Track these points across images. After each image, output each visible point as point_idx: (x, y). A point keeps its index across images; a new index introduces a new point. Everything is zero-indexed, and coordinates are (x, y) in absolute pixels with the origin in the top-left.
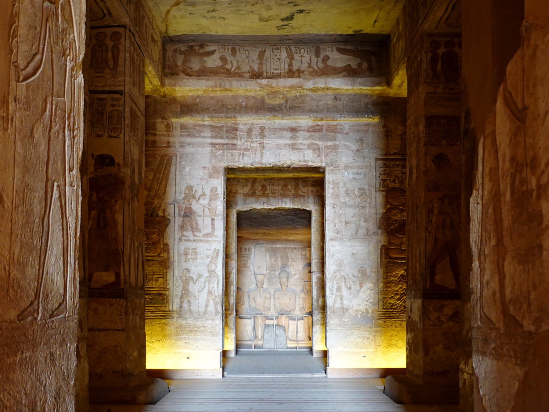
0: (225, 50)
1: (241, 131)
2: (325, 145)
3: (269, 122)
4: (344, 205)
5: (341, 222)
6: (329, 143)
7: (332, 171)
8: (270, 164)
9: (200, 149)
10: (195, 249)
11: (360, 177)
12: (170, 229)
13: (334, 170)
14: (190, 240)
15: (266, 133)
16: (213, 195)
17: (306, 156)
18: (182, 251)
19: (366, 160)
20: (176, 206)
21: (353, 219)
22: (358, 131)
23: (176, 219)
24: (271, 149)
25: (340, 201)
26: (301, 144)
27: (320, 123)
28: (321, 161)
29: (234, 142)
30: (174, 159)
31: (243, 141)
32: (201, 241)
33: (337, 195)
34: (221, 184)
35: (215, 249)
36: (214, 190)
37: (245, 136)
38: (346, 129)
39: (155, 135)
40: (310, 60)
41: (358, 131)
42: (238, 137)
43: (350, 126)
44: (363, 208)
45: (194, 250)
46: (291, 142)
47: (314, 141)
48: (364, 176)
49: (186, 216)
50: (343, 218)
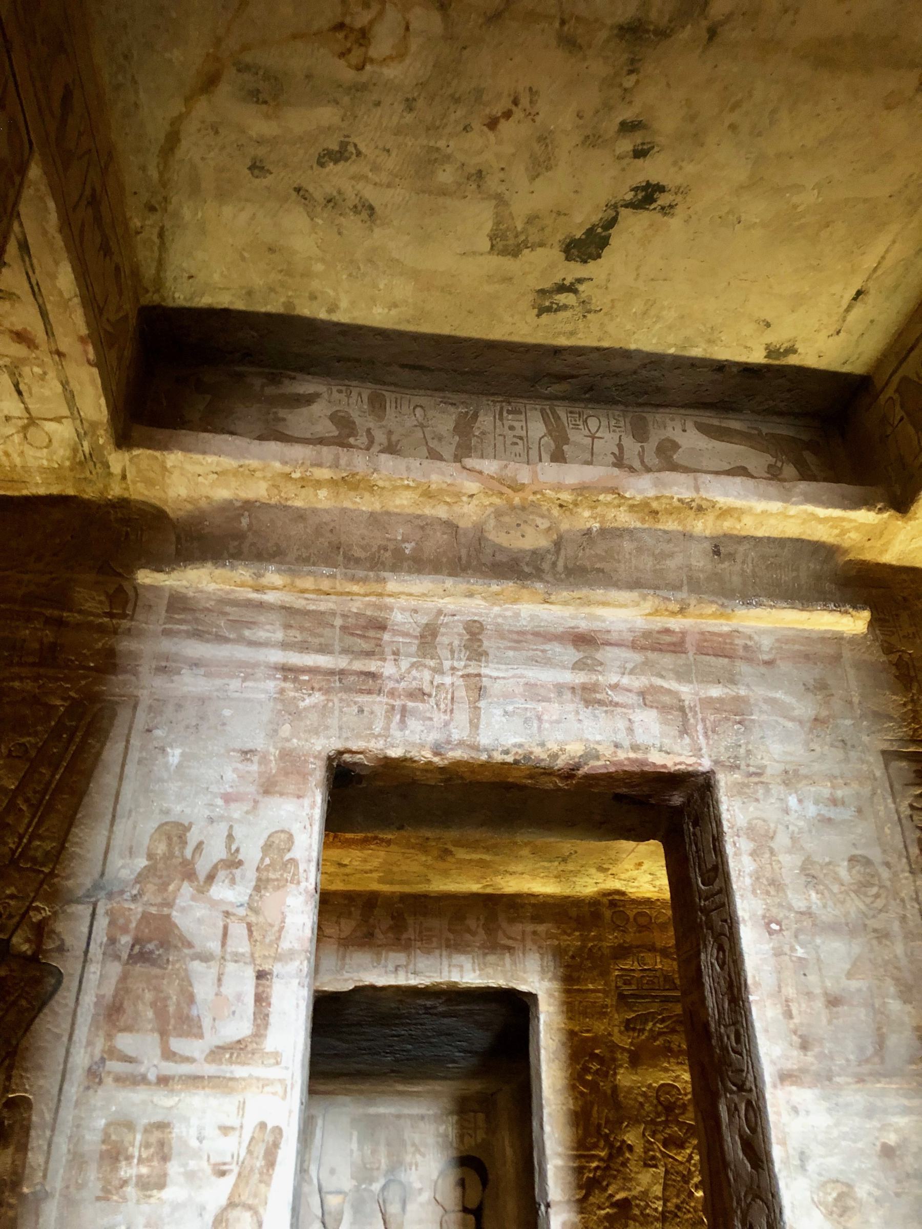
0: (349, 396)
1: (395, 633)
2: (702, 694)
3: (496, 609)
4: (807, 923)
5: (809, 995)
6: (716, 692)
7: (740, 789)
8: (507, 752)
9: (235, 684)
10: (162, 1126)
11: (847, 814)
12: (51, 1023)
13: (747, 786)
14: (143, 1080)
15: (486, 643)
17: (639, 731)
18: (92, 1139)
19: (853, 754)
20: (100, 910)
21: (854, 984)
23: (94, 970)
24: (508, 696)
25: (790, 908)
26: (615, 687)
27: (676, 624)
28: (697, 751)
29: (372, 666)
30: (123, 715)
31: (405, 664)
32: (195, 1080)
34: (310, 818)
35: (263, 1126)
36: (278, 846)
37: (414, 649)
38: (765, 648)
39: (60, 623)
40: (620, 447)
41: (807, 657)
42: (388, 650)
43: (777, 640)
44: (882, 935)
45: (156, 1135)
46: (580, 678)
48: (859, 811)
49: (140, 955)
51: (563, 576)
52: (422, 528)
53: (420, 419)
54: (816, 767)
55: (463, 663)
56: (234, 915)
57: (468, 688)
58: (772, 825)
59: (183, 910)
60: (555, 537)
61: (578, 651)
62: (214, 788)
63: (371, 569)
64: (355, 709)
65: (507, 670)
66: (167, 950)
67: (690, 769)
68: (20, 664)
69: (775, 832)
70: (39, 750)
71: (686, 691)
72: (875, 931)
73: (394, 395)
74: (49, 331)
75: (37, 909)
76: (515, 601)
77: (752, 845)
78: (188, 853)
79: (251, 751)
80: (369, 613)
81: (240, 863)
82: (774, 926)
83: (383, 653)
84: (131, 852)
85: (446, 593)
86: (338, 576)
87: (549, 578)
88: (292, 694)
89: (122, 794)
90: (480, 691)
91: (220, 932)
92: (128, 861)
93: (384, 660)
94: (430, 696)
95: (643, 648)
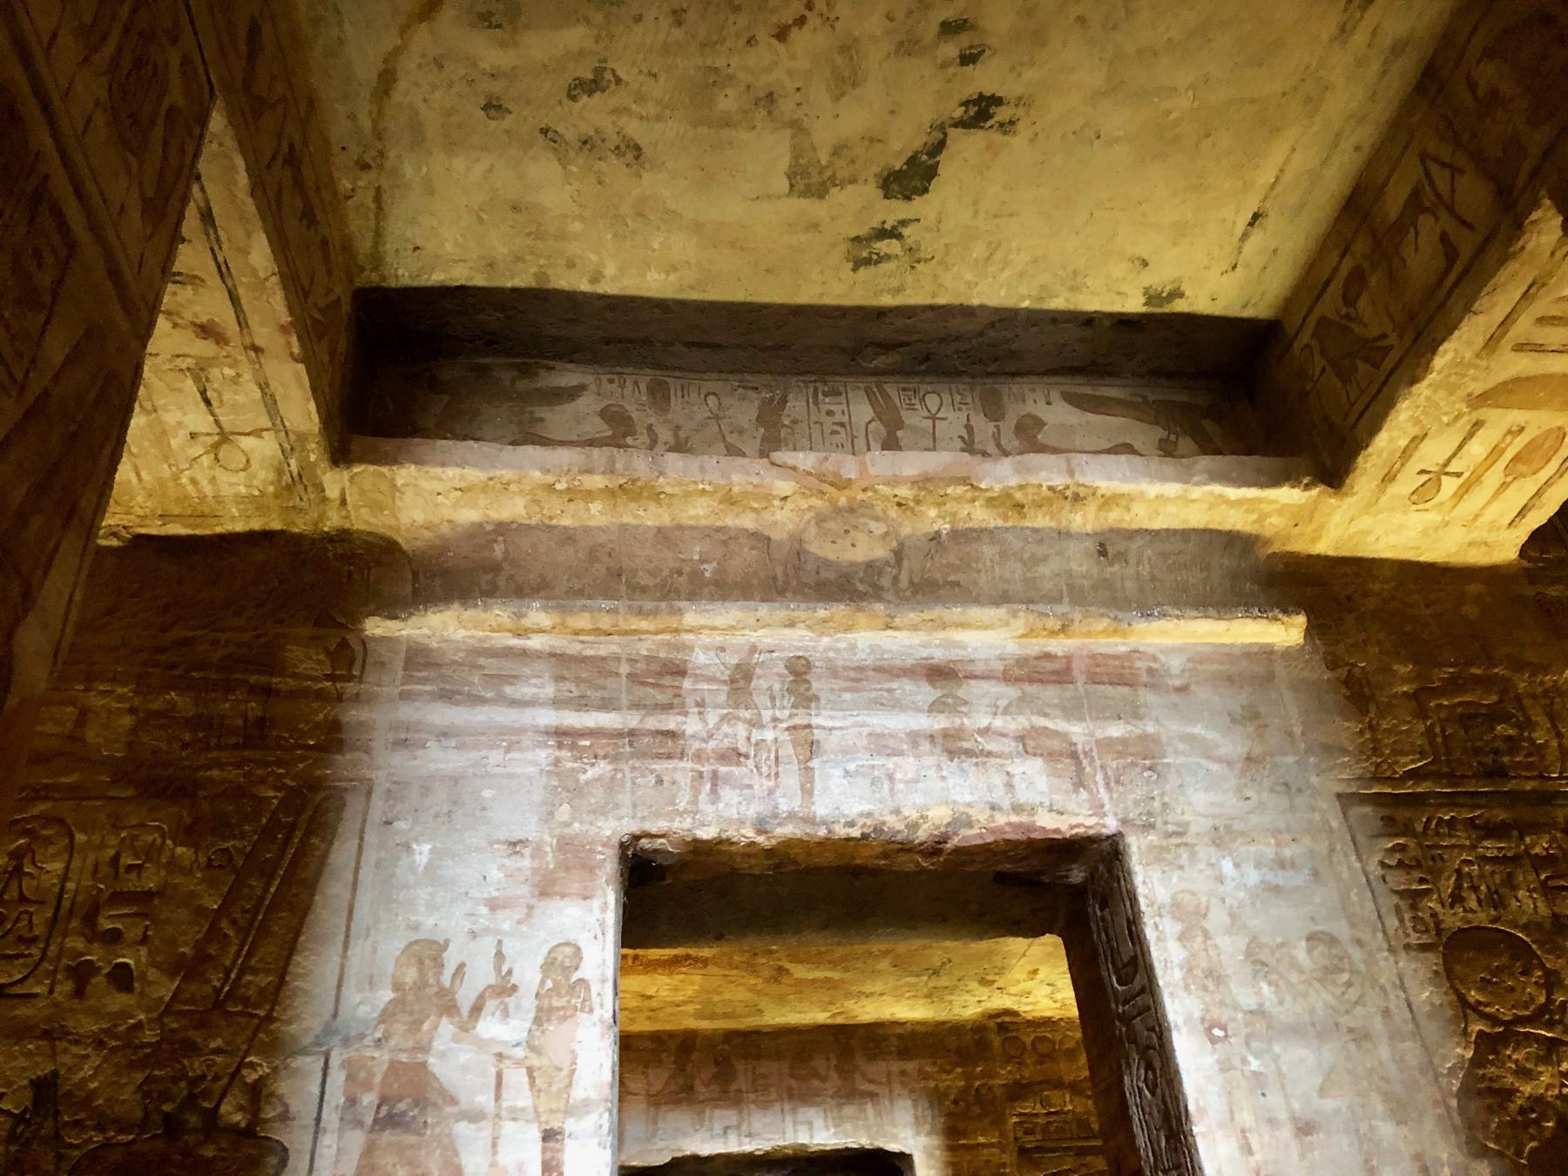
1: (698, 678)
2: (1099, 734)
3: (825, 640)
5: (1272, 1122)
6: (1116, 730)
7: (1158, 855)
8: (851, 824)
9: (495, 756)
11: (1299, 878)
13: (1168, 850)
15: (815, 685)
16: (556, 990)
17: (1020, 787)
19: (1299, 801)
20: (335, 1062)
22: (1229, 679)
23: (329, 1142)
25: (1236, 1007)
26: (985, 732)
27: (1058, 646)
28: (1098, 810)
29: (671, 722)
30: (354, 804)
31: (712, 717)
33: (1209, 974)
34: (602, 924)
36: (562, 964)
37: (723, 698)
38: (1175, 671)
39: (268, 692)
40: (969, 428)
41: (1229, 679)
42: (689, 701)
44: (1361, 1036)
47: (1041, 722)
48: (1316, 874)
50: (1274, 1099)
51: (908, 593)
52: (725, 543)
53: (715, 409)
54: (1254, 819)
55: (787, 712)
56: (509, 1057)
57: (795, 744)
58: (1204, 899)
59: (442, 1055)
60: (895, 544)
61: (934, 687)
62: (475, 893)
63: (663, 598)
64: (652, 779)
65: (844, 718)
66: (423, 1110)
67: (1091, 832)
68: (218, 747)
69: (1207, 908)
70: (248, 856)
71: (1077, 731)
72: (1351, 1030)
73: (679, 382)
74: (242, 322)
75: (252, 1066)
76: (849, 629)
77: (1178, 927)
78: (446, 979)
79: (521, 841)
80: (662, 655)
81: (514, 988)
82: (1217, 1032)
83: (683, 705)
84: (372, 982)
85: (761, 624)
86: (621, 610)
87: (890, 596)
88: (570, 765)
89: (357, 905)
90: (812, 747)
91: (492, 1081)
92: (368, 995)
93: (686, 714)
94: (747, 756)
95: (1019, 680)
